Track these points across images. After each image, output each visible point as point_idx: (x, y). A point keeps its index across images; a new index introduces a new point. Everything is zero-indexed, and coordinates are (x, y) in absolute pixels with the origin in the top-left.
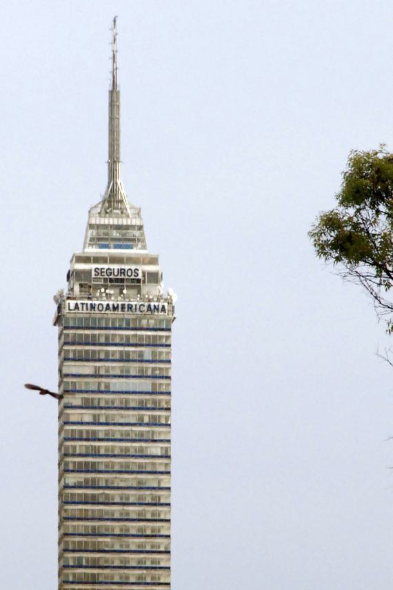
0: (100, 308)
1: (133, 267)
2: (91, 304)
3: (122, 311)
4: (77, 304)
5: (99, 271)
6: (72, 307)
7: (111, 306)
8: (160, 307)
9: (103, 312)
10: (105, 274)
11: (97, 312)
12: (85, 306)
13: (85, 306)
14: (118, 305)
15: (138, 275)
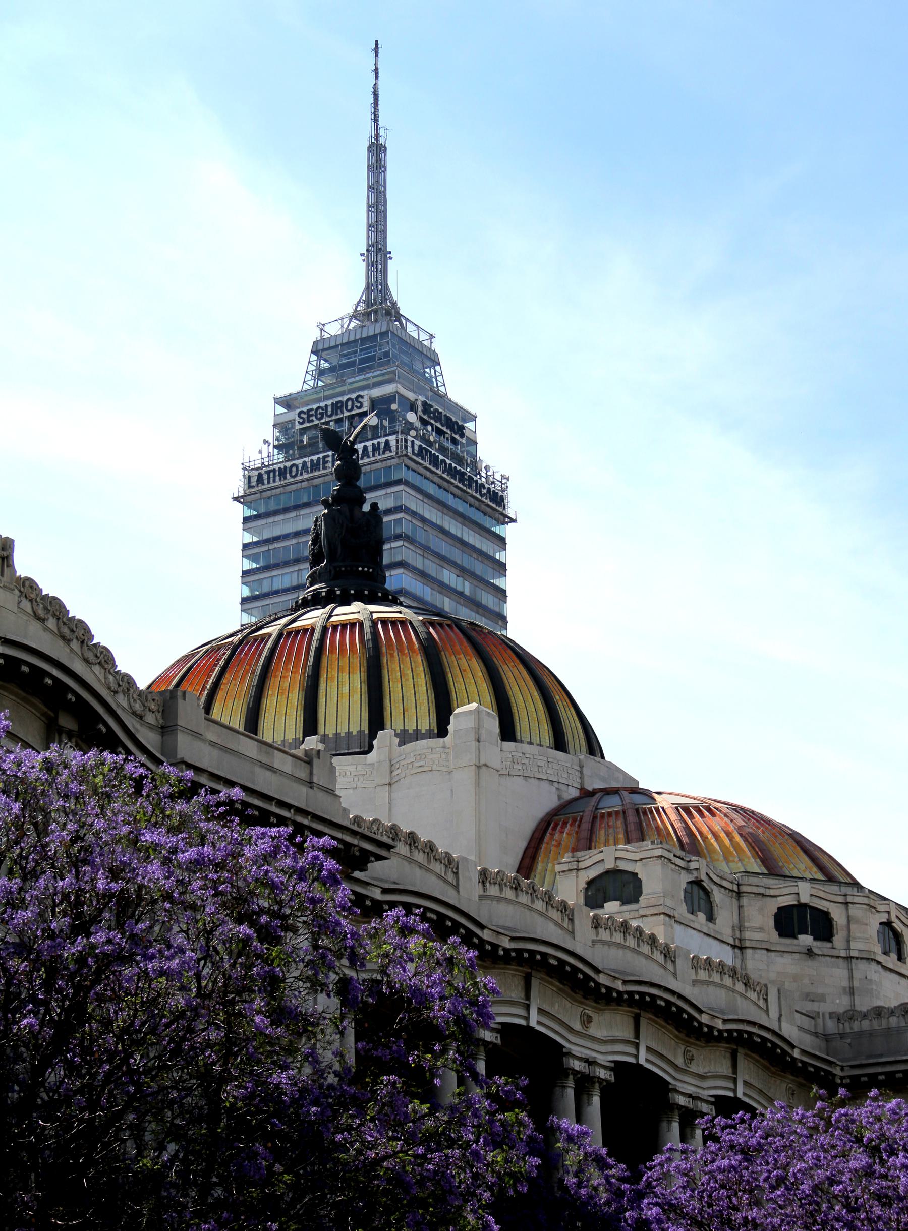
0: (294, 469)
1: (354, 396)
2: (280, 468)
3: (325, 468)
4: (260, 476)
5: (305, 416)
6: (254, 479)
7: (309, 465)
8: (382, 446)
9: (299, 478)
10: (314, 418)
11: (290, 480)
12: (272, 475)
13: (272, 475)
14: (319, 458)
15: (362, 404)
